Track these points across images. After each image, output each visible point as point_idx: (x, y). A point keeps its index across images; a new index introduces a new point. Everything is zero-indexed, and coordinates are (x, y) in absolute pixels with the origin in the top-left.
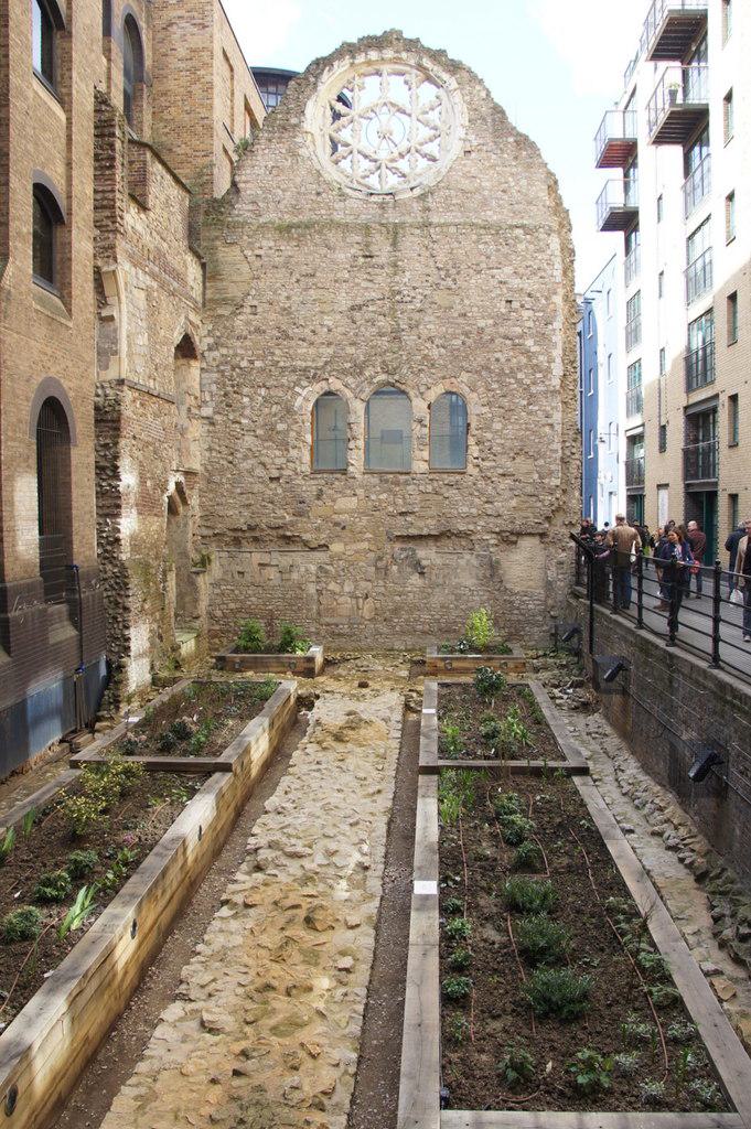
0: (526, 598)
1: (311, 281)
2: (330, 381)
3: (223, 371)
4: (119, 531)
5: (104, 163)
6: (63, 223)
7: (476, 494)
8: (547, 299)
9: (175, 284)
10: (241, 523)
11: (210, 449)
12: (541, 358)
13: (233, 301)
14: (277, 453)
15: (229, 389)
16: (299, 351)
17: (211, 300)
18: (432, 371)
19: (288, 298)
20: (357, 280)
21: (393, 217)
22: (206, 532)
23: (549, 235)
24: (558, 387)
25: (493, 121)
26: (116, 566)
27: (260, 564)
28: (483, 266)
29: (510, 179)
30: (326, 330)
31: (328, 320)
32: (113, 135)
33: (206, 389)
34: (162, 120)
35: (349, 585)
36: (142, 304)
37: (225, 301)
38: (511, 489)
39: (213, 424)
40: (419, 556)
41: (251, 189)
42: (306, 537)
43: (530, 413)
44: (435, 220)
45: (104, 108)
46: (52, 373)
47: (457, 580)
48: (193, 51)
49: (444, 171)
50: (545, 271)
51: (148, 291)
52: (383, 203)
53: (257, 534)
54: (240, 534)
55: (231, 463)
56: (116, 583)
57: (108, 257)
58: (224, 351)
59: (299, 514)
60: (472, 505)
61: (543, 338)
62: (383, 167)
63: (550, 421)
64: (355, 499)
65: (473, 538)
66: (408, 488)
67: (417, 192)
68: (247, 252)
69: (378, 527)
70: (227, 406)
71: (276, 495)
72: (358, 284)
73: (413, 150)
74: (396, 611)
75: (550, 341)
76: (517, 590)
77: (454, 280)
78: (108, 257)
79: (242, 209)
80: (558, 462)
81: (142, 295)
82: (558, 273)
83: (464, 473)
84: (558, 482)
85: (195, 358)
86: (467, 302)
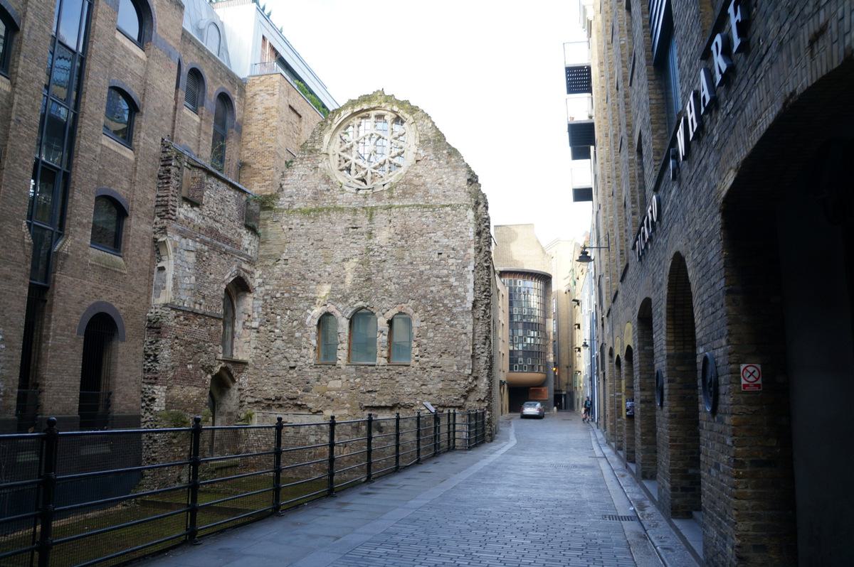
1: (320, 244)
2: (328, 306)
3: (266, 300)
4: (154, 392)
5: (164, 178)
6: (127, 215)
7: (417, 379)
8: (464, 251)
9: (228, 247)
10: (272, 395)
11: (254, 348)
12: (460, 289)
13: (274, 255)
14: (295, 351)
15: (269, 310)
16: (311, 287)
17: (262, 256)
18: (390, 299)
19: (306, 254)
20: (348, 243)
21: (371, 203)
23: (467, 210)
24: (470, 309)
25: (437, 143)
26: (152, 414)
28: (424, 231)
29: (444, 176)
30: (327, 274)
31: (329, 269)
32: (171, 165)
33: (256, 310)
34: (248, 149)
36: (191, 258)
37: (270, 257)
38: (439, 377)
39: (258, 332)
41: (289, 188)
42: (310, 405)
43: (452, 326)
44: (397, 203)
45: (167, 150)
46: (105, 298)
48: (266, 109)
49: (404, 173)
50: (463, 233)
51: (199, 255)
52: (366, 194)
53: (281, 402)
54: (271, 402)
55: (267, 356)
56: (151, 425)
57: (163, 233)
58: (268, 287)
59: (306, 390)
60: (413, 386)
61: (461, 276)
62: (369, 173)
63: (465, 331)
64: (340, 381)
66: (374, 375)
67: (386, 187)
68: (285, 227)
70: (268, 321)
71: (293, 378)
72: (347, 245)
73: (387, 161)
75: (466, 278)
77: (406, 241)
78: (163, 233)
79: (283, 202)
80: (470, 358)
81: (193, 255)
82: (471, 233)
83: (409, 366)
84: (470, 372)
85: (250, 292)
86: (413, 255)
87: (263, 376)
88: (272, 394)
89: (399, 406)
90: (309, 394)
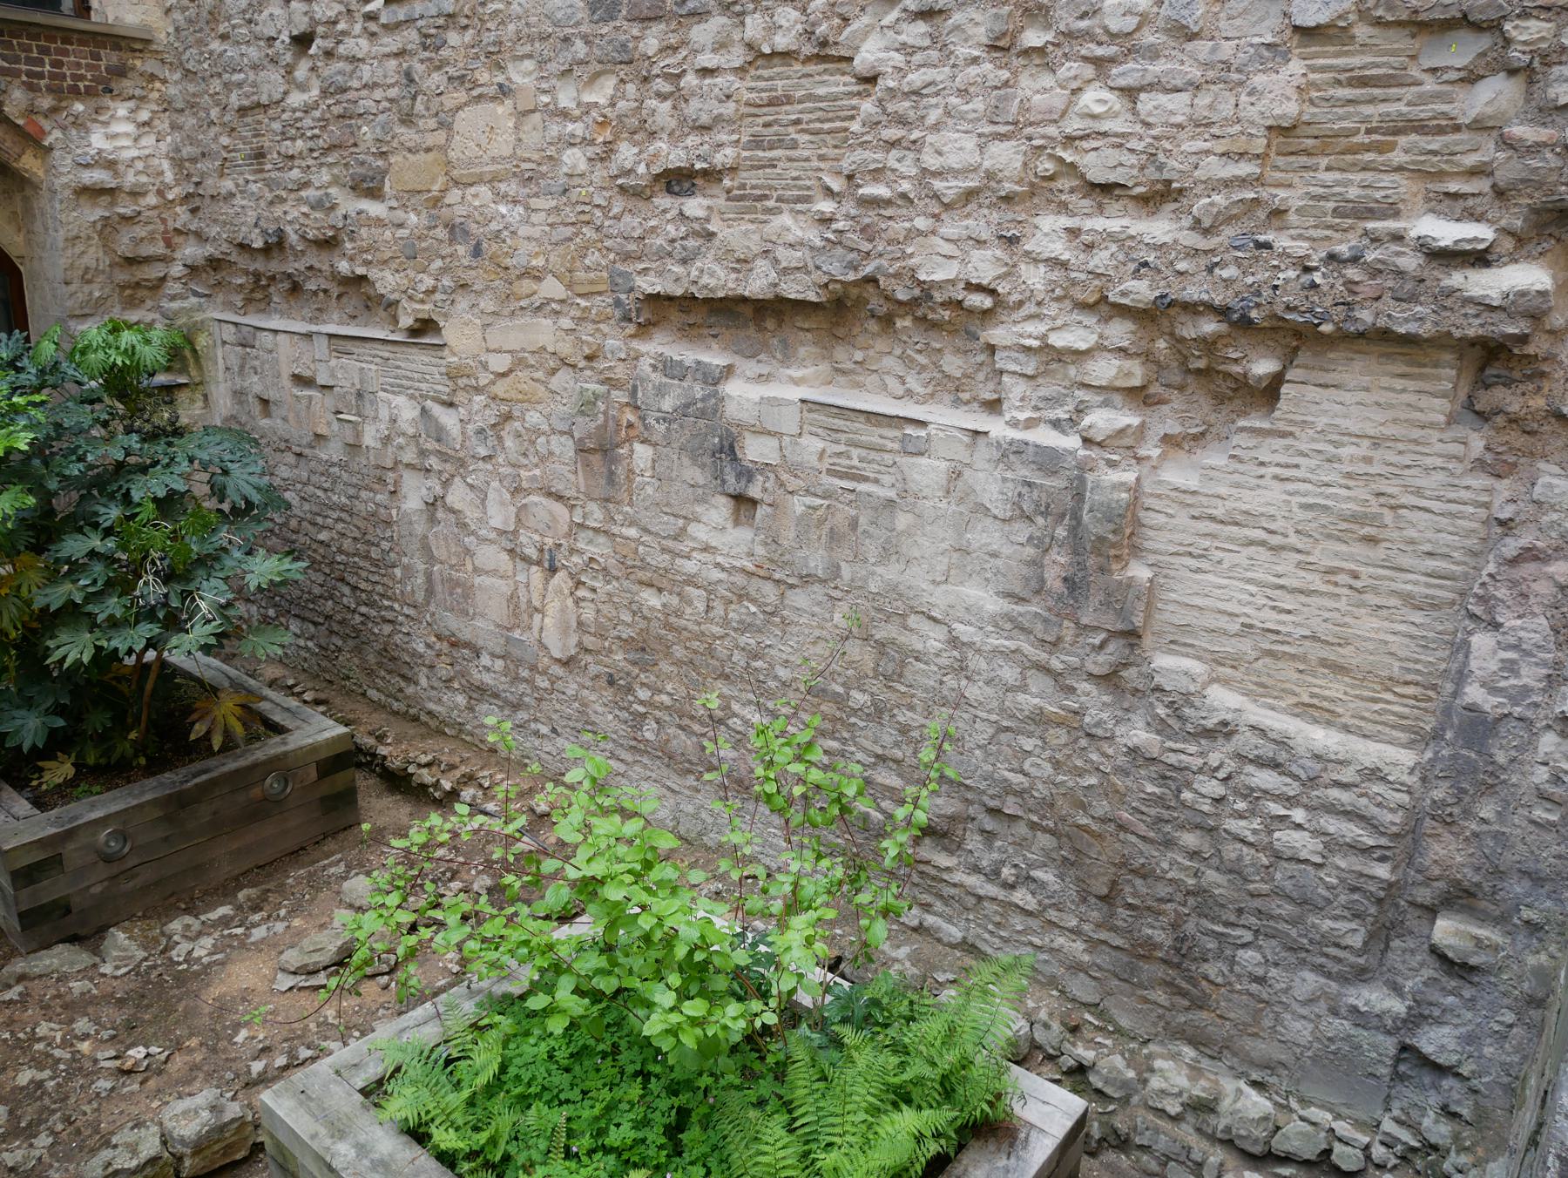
0: (1265, 779)
7: (1033, 38)
22: (191, 251)
27: (301, 380)
35: (502, 503)
40: (731, 411)
47: (890, 572)
64: (503, 109)
65: (998, 334)
69: (583, 252)
74: (642, 649)
76: (1224, 700)
87: (214, 113)
88: (251, 217)
89: (876, 303)
90: (374, 208)
